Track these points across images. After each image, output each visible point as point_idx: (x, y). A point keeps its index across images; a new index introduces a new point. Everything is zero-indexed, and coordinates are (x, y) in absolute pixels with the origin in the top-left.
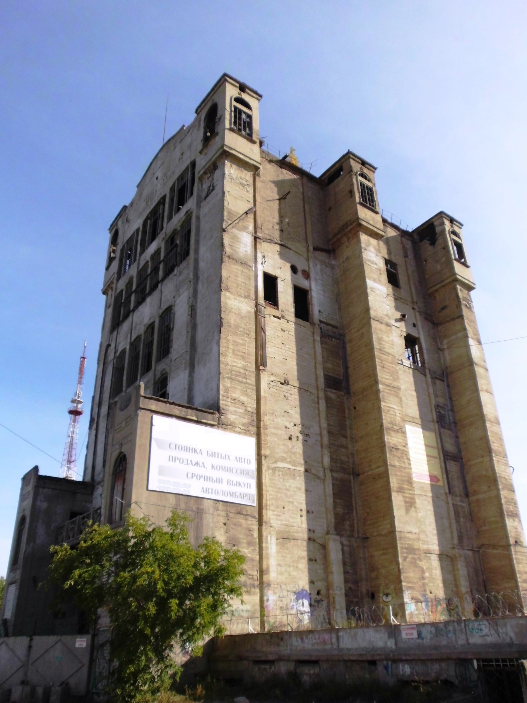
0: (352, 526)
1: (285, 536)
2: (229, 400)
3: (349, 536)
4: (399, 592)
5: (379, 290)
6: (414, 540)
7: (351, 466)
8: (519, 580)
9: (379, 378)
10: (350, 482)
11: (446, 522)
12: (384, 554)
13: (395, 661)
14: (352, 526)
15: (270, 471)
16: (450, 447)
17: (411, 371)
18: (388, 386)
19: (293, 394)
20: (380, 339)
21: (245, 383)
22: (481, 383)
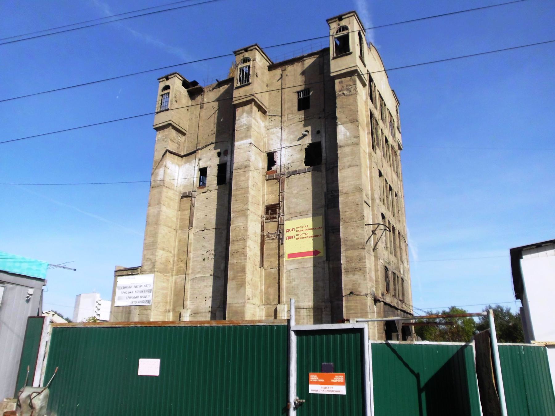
5: (244, 144)
20: (236, 182)
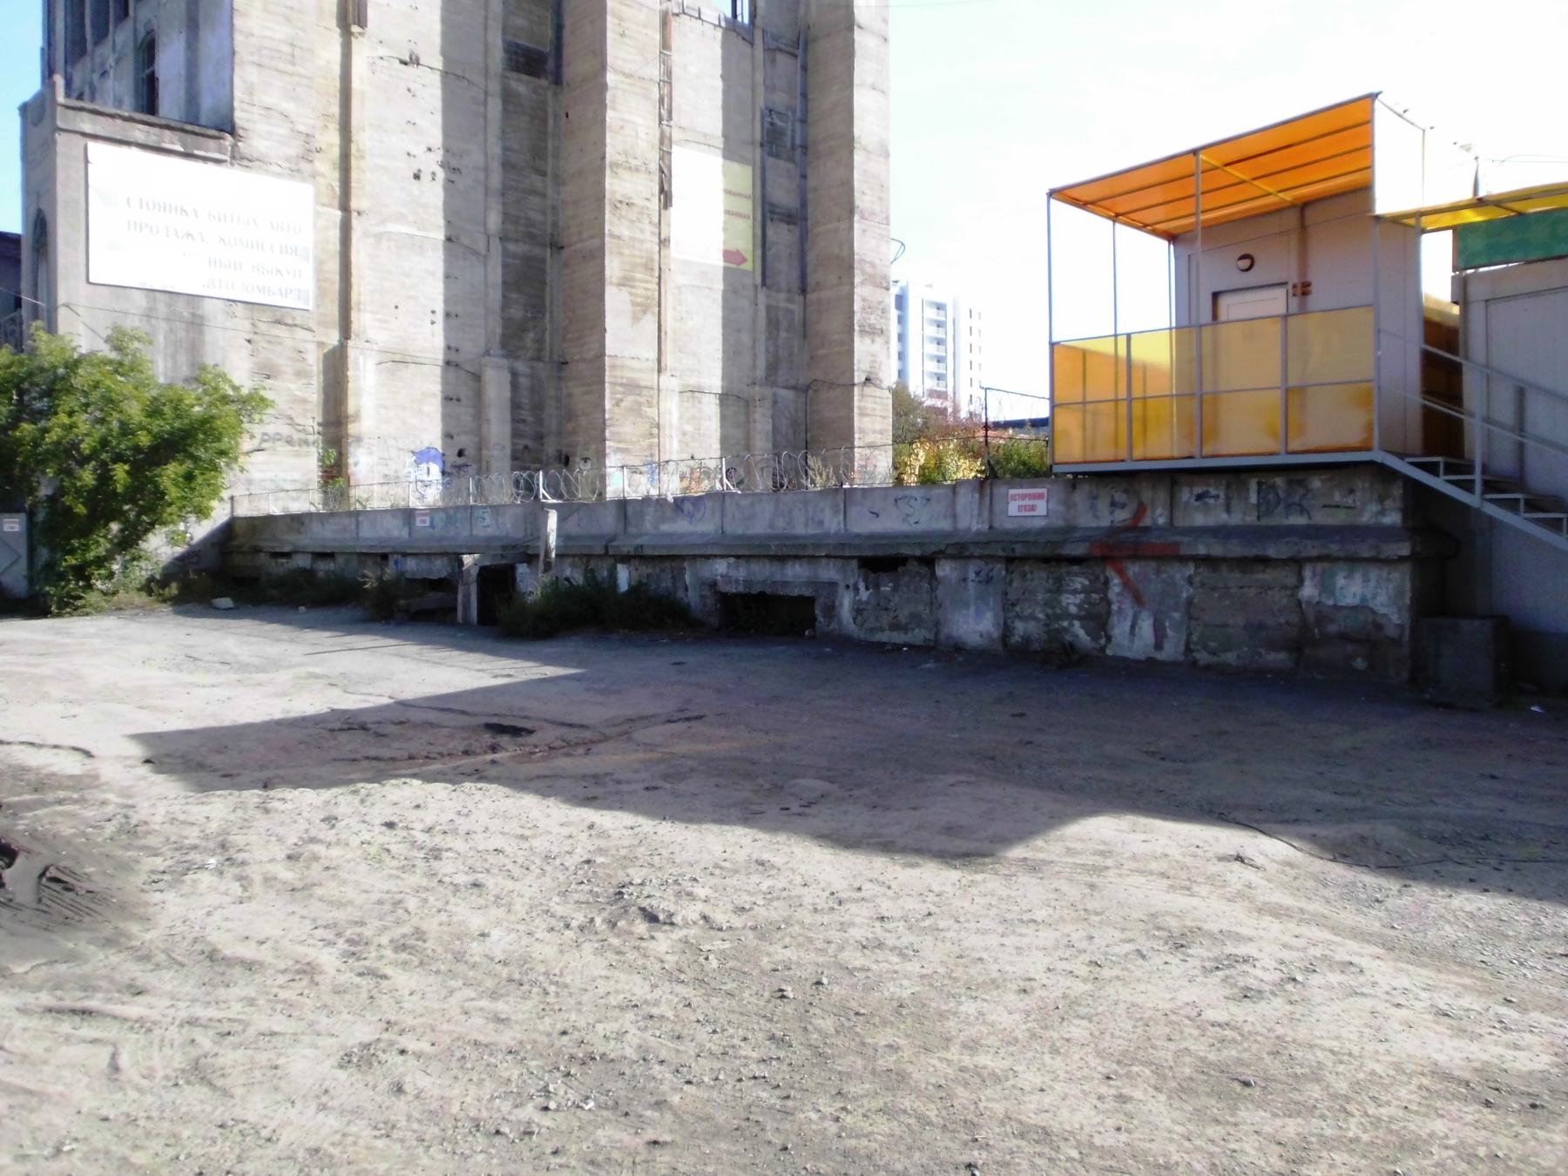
0: (540, 341)
1: (397, 358)
2: (255, 109)
3: (532, 359)
4: (601, 455)
6: (641, 371)
7: (549, 231)
8: (857, 443)
9: (609, 60)
10: (543, 261)
11: (746, 339)
12: (587, 393)
13: (405, 555)
14: (540, 341)
15: (371, 240)
16: (784, 196)
17: (719, 34)
18: (630, 76)
19: (429, 87)
21: (292, 74)
22: (863, 70)
